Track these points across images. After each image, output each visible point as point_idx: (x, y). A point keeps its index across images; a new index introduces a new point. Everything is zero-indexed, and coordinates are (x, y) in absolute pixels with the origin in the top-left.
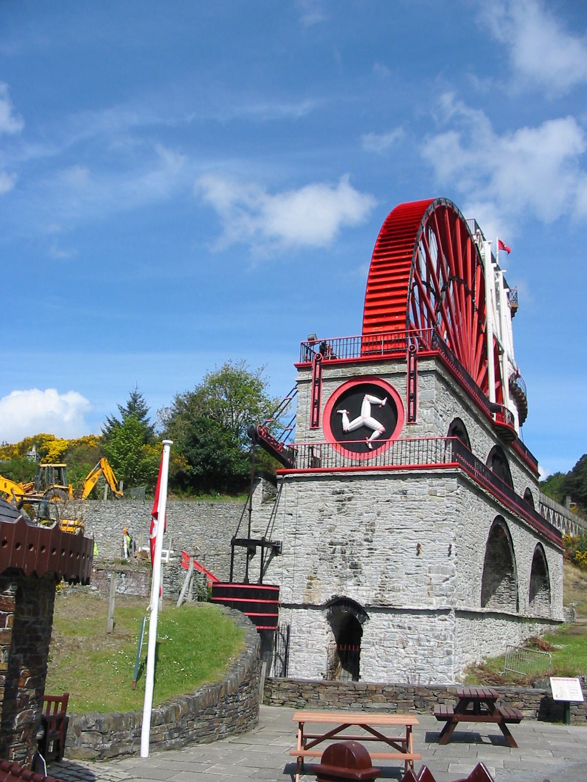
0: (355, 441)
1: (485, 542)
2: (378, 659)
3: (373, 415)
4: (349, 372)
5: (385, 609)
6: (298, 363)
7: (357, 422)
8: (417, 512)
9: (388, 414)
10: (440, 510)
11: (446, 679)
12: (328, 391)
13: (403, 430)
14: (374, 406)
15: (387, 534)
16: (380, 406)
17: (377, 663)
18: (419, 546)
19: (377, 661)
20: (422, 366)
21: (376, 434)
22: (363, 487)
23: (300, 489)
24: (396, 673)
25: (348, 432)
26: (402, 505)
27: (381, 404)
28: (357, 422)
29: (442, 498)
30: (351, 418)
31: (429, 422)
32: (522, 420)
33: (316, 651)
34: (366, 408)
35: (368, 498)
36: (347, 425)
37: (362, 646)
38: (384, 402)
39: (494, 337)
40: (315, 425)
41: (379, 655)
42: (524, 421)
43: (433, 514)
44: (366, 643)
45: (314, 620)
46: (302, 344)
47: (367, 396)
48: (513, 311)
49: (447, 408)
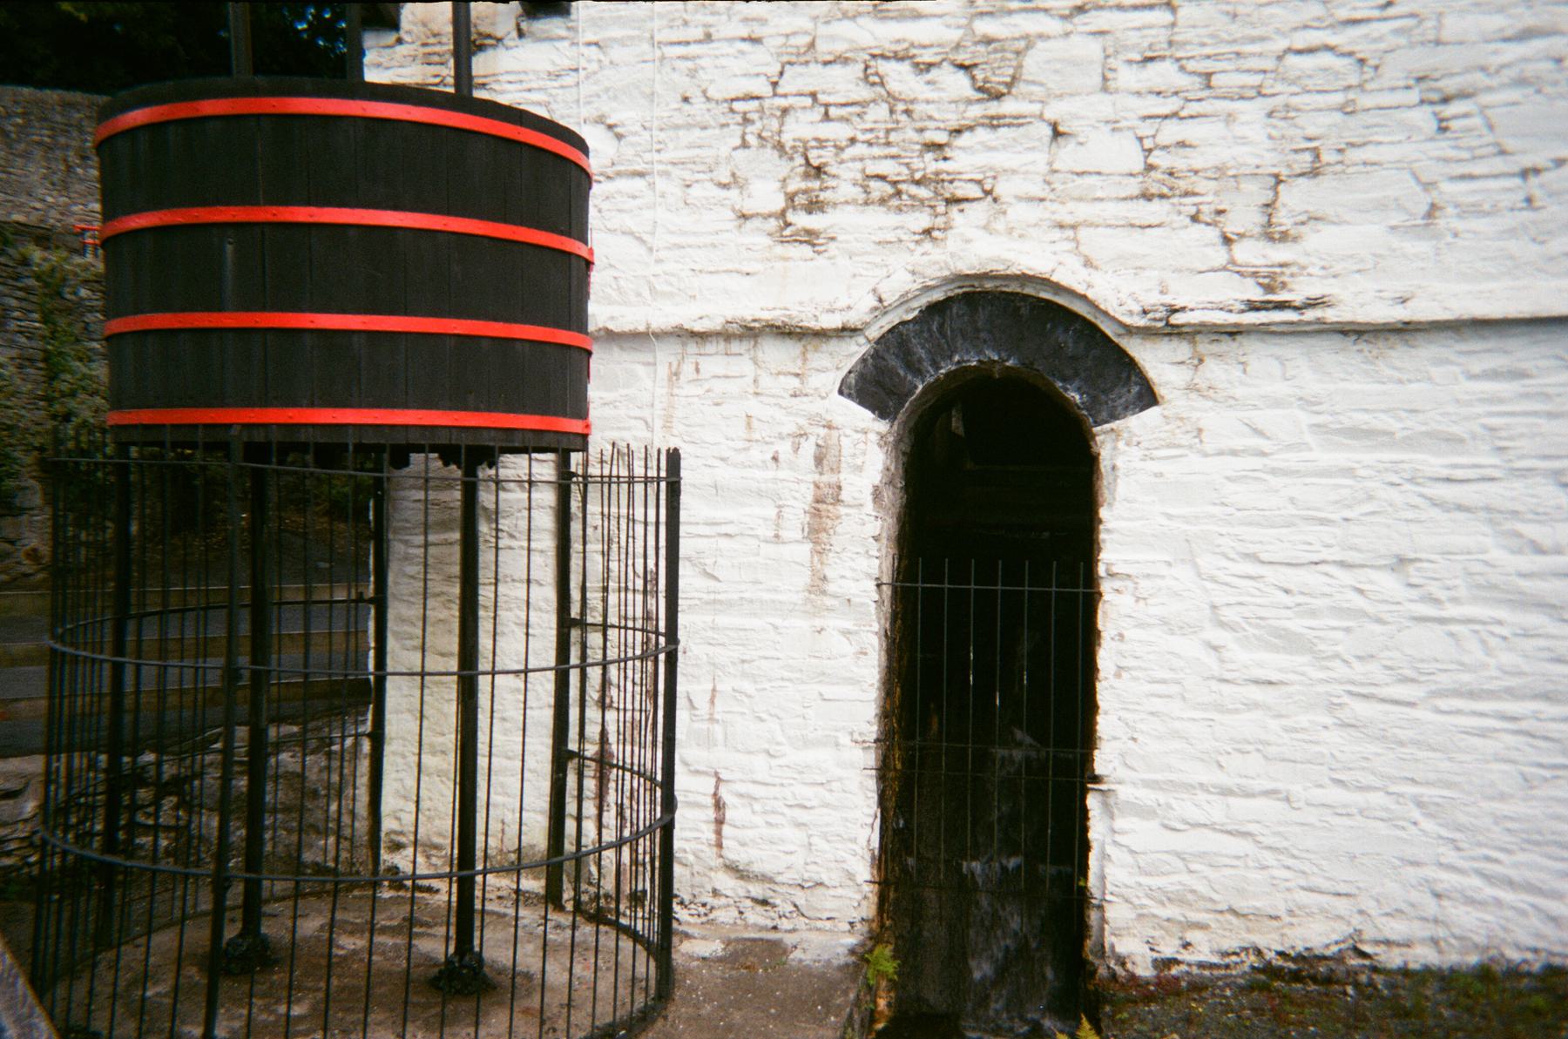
5: (1280, 319)
17: (1210, 659)
24: (1344, 715)
41: (1229, 614)
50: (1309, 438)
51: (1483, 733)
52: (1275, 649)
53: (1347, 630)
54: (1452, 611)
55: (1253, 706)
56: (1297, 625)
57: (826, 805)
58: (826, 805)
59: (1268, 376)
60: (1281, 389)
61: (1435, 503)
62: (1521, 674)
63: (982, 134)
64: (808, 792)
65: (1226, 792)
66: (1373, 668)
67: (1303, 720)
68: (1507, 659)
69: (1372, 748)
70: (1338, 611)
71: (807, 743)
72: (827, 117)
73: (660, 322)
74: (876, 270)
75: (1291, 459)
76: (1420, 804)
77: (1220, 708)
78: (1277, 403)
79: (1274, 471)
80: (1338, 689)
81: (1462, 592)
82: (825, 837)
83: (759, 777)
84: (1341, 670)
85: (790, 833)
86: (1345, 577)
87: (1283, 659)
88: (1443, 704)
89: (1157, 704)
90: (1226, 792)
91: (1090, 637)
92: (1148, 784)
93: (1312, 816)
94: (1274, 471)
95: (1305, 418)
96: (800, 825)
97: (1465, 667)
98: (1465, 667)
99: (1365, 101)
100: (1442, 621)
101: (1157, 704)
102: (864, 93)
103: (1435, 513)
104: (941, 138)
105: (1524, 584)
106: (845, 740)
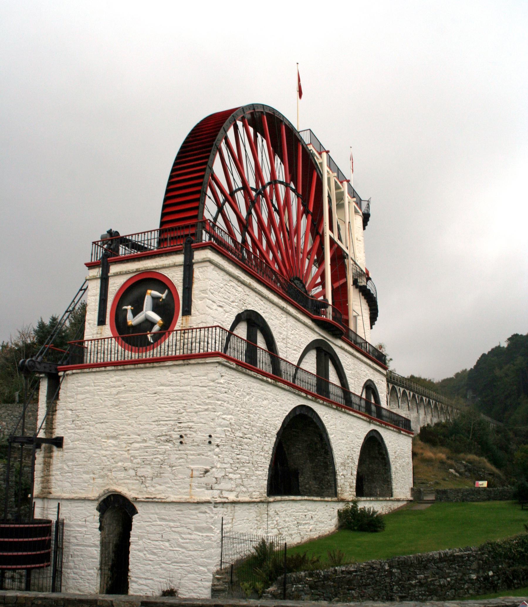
0: (133, 337)
1: (275, 432)
2: (145, 552)
3: (156, 308)
6: (89, 261)
7: (140, 317)
8: (181, 403)
10: (203, 400)
11: (206, 573)
13: (180, 322)
14: (154, 298)
15: (154, 426)
16: (161, 300)
17: (144, 556)
18: (181, 437)
19: (145, 554)
20: (198, 255)
21: (156, 328)
22: (134, 380)
23: (79, 384)
25: (132, 326)
26: (167, 397)
27: (160, 298)
28: (140, 317)
30: (135, 313)
31: (203, 312)
32: (373, 317)
33: (92, 545)
34: (148, 302)
35: (137, 391)
36: (132, 320)
38: (164, 296)
39: (332, 241)
40: (101, 322)
41: (147, 549)
42: (376, 320)
43: (195, 405)
44: (135, 536)
45: (89, 514)
46: (94, 243)
47: (149, 291)
48: (366, 218)
49: (231, 300)
50: (157, 520)
51: (178, 569)
52: (152, 554)
54: (174, 549)
55: (149, 564)
56: (155, 551)
59: (152, 508)
60: (153, 511)
61: (173, 531)
63: (116, 469)
64: (90, 577)
65: (146, 579)
67: (156, 567)
68: (181, 557)
69: (164, 572)
71: (89, 569)
73: (71, 497)
74: (96, 491)
75: (155, 523)
77: (145, 565)
78: (153, 514)
79: (152, 525)
80: (160, 562)
82: (92, 585)
84: (161, 559)
85: (87, 584)
86: (162, 543)
88: (173, 564)
89: (137, 564)
90: (146, 579)
91: (128, 552)
92: (136, 577)
93: (156, 583)
94: (152, 525)
95: (156, 516)
96: (88, 583)
97: (176, 558)
98: (176, 558)
100: (173, 550)
101: (137, 564)
103: (173, 533)
105: (182, 544)
106: (95, 568)
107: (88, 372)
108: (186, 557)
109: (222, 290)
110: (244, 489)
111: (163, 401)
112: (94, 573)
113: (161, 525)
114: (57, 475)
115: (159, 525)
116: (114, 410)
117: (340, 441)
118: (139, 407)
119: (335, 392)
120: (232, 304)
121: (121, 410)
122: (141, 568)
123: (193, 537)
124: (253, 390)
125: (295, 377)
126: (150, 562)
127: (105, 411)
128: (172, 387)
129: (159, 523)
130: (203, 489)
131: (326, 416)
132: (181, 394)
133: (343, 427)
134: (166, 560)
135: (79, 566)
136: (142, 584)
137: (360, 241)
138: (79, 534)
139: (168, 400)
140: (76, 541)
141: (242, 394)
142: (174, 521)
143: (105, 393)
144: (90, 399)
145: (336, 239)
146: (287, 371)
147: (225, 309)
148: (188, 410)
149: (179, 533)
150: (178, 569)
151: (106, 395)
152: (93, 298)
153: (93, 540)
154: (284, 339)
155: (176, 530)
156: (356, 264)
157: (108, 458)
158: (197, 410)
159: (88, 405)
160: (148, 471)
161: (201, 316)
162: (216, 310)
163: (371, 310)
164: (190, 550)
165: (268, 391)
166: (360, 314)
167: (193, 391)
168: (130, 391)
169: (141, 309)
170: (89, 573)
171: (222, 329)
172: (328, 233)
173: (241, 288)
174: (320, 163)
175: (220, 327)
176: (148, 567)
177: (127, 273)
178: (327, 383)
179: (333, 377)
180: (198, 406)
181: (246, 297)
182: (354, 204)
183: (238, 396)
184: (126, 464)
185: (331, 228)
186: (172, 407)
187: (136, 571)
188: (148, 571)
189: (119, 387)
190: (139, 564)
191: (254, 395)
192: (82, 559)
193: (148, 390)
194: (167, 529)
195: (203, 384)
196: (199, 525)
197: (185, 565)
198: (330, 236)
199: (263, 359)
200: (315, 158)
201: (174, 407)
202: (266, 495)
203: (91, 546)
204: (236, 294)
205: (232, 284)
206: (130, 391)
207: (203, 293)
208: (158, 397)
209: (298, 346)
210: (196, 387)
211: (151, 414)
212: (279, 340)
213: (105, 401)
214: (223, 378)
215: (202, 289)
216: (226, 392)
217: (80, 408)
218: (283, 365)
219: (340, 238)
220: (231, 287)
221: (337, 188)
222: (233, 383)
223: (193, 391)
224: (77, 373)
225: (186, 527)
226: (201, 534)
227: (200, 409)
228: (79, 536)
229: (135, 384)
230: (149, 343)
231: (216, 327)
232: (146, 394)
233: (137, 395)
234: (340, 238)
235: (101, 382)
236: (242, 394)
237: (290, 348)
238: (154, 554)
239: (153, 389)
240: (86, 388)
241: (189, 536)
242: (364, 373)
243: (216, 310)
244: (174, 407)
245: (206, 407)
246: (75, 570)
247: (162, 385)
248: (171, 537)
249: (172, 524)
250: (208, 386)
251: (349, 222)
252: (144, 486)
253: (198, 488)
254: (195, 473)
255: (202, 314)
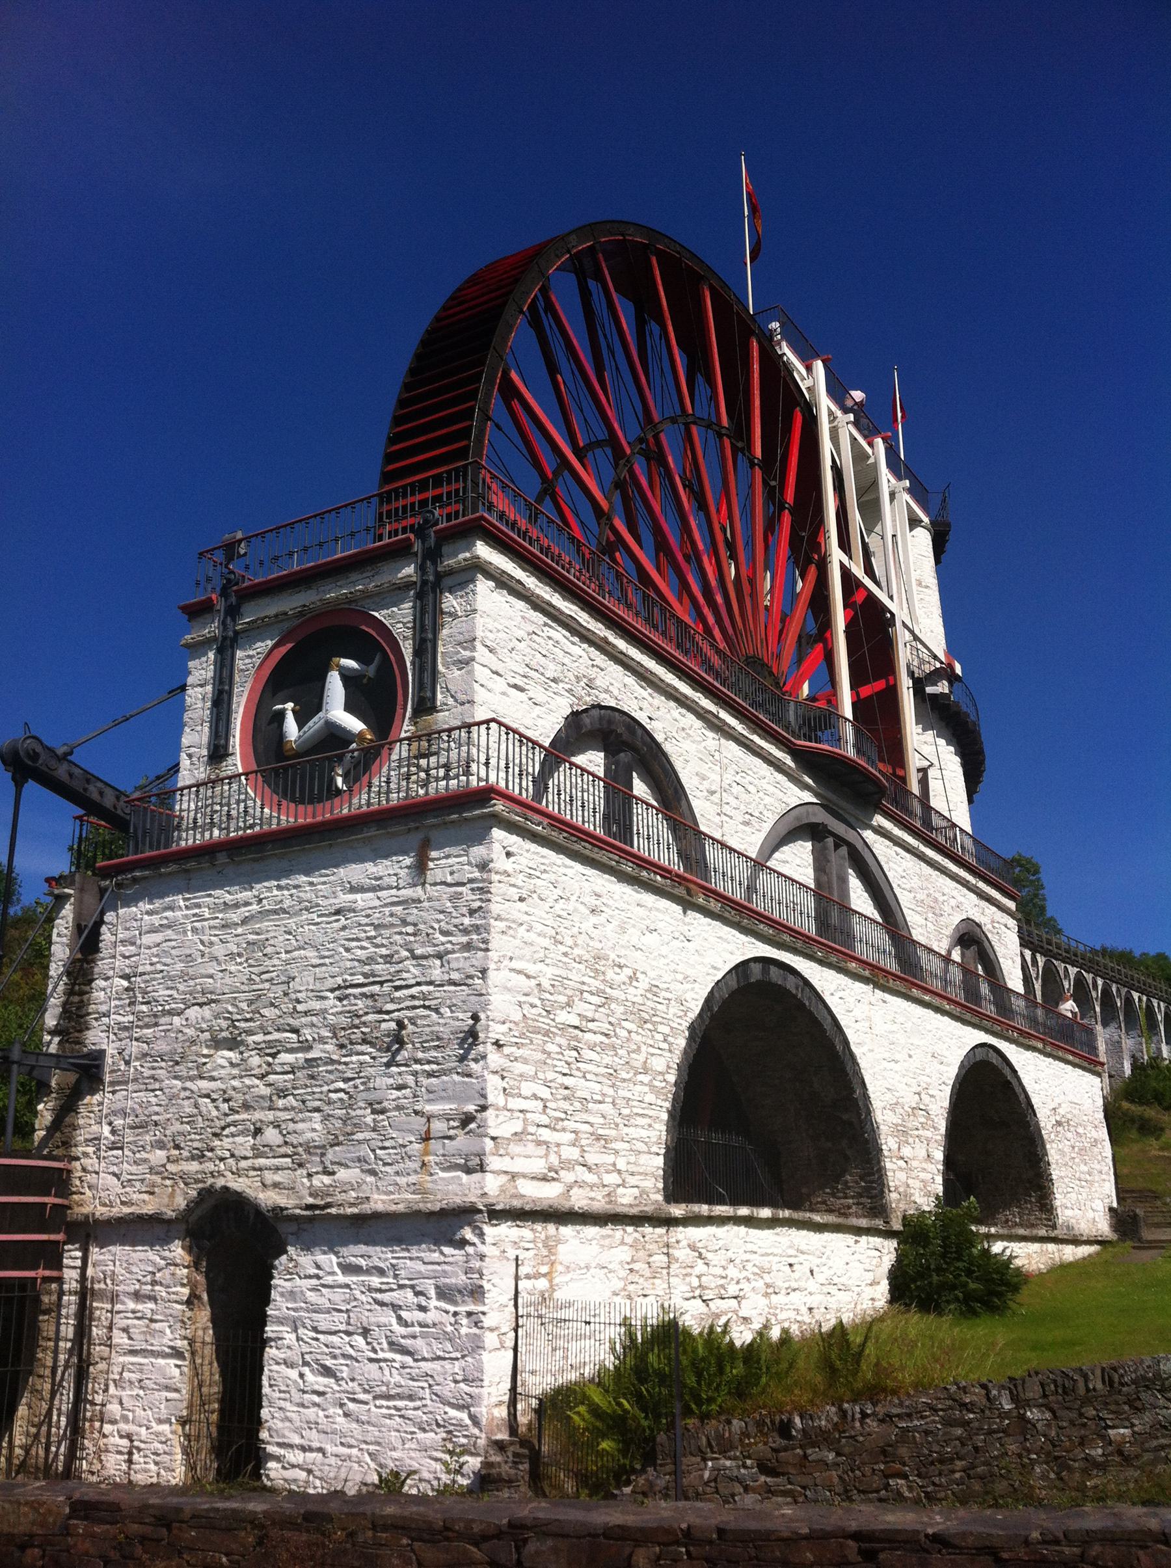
4: (290, 603)
9: (375, 698)
12: (251, 658)
14: (348, 679)
16: (365, 681)
18: (401, 1025)
26: (366, 921)
29: (460, 889)
33: (167, 1350)
34: (335, 687)
35: (292, 911)
37: (270, 1330)
38: (371, 671)
40: (218, 753)
43: (437, 935)
44: (280, 1321)
51: (390, 1417)
52: (322, 1375)
53: (347, 1365)
56: (329, 1362)
57: (165, 1453)
58: (165, 1453)
61: (377, 1302)
62: (401, 1386)
63: (232, 1129)
66: (355, 1384)
70: (344, 1356)
71: (160, 1421)
72: (182, 1123)
76: (370, 1454)
77: (303, 1406)
79: (324, 1286)
80: (343, 1395)
81: (385, 1346)
83: (143, 1438)
86: (347, 1339)
87: (326, 1380)
88: (378, 1403)
89: (282, 1404)
92: (279, 1445)
94: (324, 1286)
99: (353, 1113)
101: (282, 1404)
102: (195, 1111)
104: (218, 1131)
105: (402, 1341)
106: (173, 1420)
107: (170, 874)
108: (413, 1379)
109: (522, 645)
110: (591, 1178)
111: (355, 931)
112: (173, 1432)
113: (347, 1286)
114: (86, 1155)
115: (340, 1286)
116: (233, 968)
117: (885, 1064)
118: (296, 954)
119: (871, 939)
120: (552, 684)
121: (250, 966)
122: (293, 1416)
123: (430, 1317)
124: (610, 902)
125: (751, 889)
126: (316, 1399)
127: (212, 971)
128: (380, 894)
129: (341, 1278)
130: (459, 1173)
131: (841, 994)
132: (400, 908)
133: (895, 1027)
134: (358, 1389)
135: (133, 1411)
136: (293, 1466)
137: (927, 587)
138: (136, 1322)
139: (367, 928)
140: (126, 1341)
141: (576, 910)
142: (381, 1272)
143: (212, 922)
144: (173, 943)
145: (858, 571)
146: (728, 876)
147: (531, 694)
148: (418, 952)
149: (396, 1308)
150: (390, 1417)
151: (215, 927)
152: (199, 689)
153: (171, 1336)
154: (713, 793)
155: (386, 1297)
156: (916, 638)
157: (214, 1101)
158: (442, 948)
159: (168, 961)
160: (314, 1130)
161: (460, 708)
162: (504, 694)
163: (965, 765)
164: (424, 1359)
165: (657, 910)
166: (936, 762)
167: (430, 899)
168: (275, 912)
169: (319, 708)
170: (157, 1434)
171: (507, 728)
172: (837, 556)
173: (580, 650)
174: (808, 389)
175: (500, 724)
176: (311, 1413)
177: (281, 617)
178: (847, 910)
179: (860, 899)
180: (443, 939)
181: (593, 673)
182: (907, 497)
183: (564, 914)
184: (258, 1115)
185: (845, 545)
186: (377, 946)
187: (280, 1425)
188: (312, 1424)
189: (247, 904)
190: (287, 1405)
191: (612, 916)
192: (141, 1393)
193: (318, 905)
194: (363, 1298)
195: (457, 877)
196: (447, 1281)
197: (411, 1404)
198: (842, 565)
199: (651, 833)
200: (795, 374)
201: (383, 945)
202: (660, 1197)
203: (165, 1356)
204: (566, 661)
205: (552, 633)
206: (275, 912)
207: (465, 649)
208: (343, 922)
209: (757, 814)
210: (438, 887)
211: (324, 968)
212: (698, 794)
213: (211, 943)
214: (512, 859)
215: (461, 638)
216: (521, 900)
217: (149, 968)
218: (713, 855)
219: (869, 571)
220: (551, 642)
221: (860, 457)
222: (544, 876)
223: (430, 899)
224: (144, 878)
225: (412, 1287)
226: (452, 1309)
227: (449, 946)
228: (135, 1326)
229: (286, 892)
230: (339, 792)
231: (487, 722)
232: (314, 916)
233: (291, 923)
234: (869, 571)
235: (203, 897)
236: (576, 910)
237: (731, 818)
238: (327, 1372)
239: (332, 901)
240: (165, 914)
241: (419, 1316)
242: (953, 902)
243: (504, 694)
244: (383, 945)
245: (465, 939)
246: (123, 1426)
247: (353, 889)
248: (373, 1320)
249: (375, 1281)
250: (471, 881)
251: (894, 536)
252: (305, 1172)
253: (444, 1170)
254: (438, 1126)
255: (462, 704)
